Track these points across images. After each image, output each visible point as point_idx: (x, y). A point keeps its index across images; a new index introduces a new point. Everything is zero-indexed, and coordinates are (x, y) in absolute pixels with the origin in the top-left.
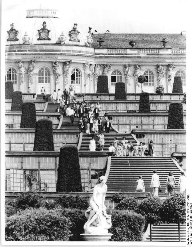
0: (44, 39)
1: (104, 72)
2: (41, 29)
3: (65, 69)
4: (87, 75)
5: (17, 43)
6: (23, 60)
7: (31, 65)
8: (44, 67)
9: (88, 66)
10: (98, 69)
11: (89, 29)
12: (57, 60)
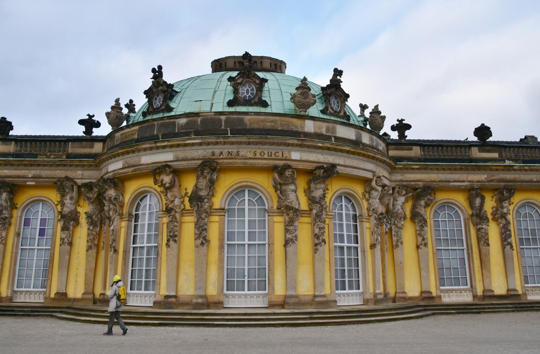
0: (247, 102)
1: (417, 210)
2: (238, 74)
3: (313, 194)
4: (377, 217)
7: (201, 180)
8: (247, 186)
11: (359, 109)
12: (289, 163)
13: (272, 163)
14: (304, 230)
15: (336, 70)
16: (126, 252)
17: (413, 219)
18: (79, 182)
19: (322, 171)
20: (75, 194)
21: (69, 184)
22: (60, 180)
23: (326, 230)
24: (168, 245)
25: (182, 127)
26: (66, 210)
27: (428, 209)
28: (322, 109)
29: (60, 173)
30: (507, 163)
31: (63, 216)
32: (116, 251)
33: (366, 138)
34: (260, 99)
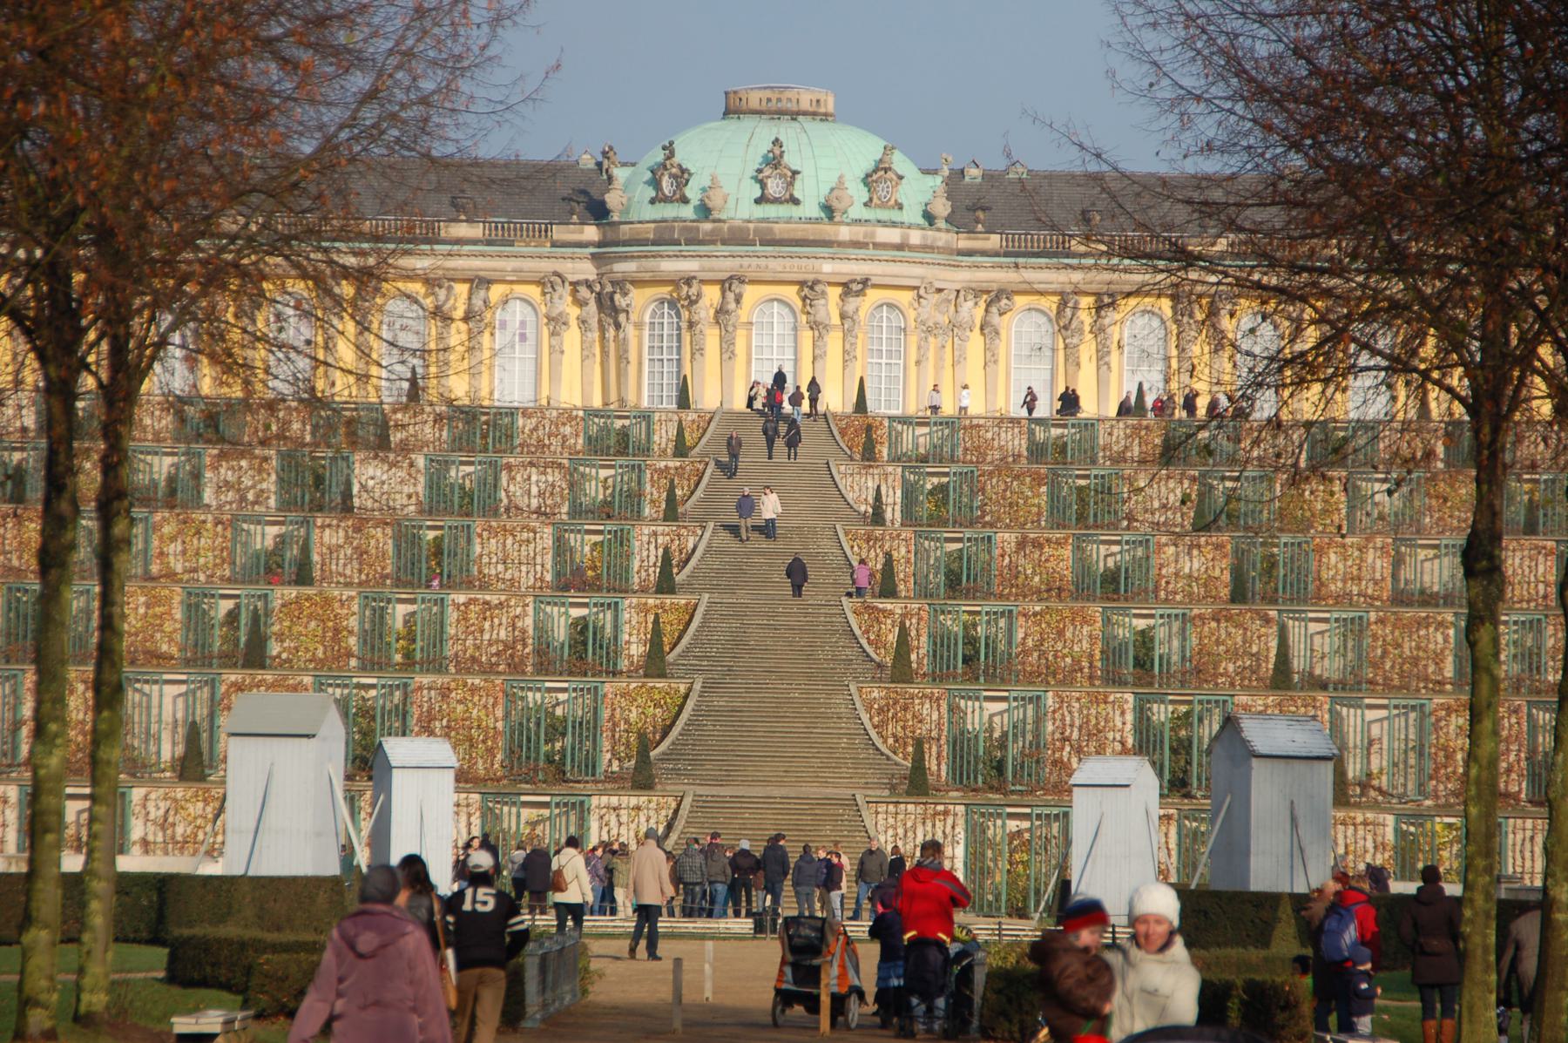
0: (776, 201)
6: (701, 276)
12: (820, 277)
13: (800, 277)
25: (706, 233)
28: (866, 199)
29: (547, 266)
31: (550, 319)
33: (915, 237)
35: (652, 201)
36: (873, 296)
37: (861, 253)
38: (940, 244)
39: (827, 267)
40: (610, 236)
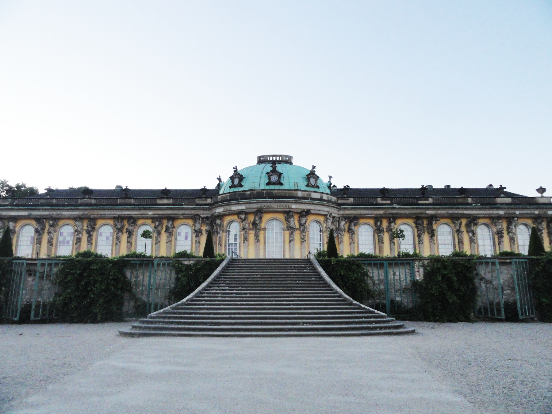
0: (274, 184)
5: (241, 189)
9: (331, 219)
10: (343, 223)
11: (328, 178)
14: (297, 235)
15: (313, 166)
16: (225, 246)
17: (348, 231)
18: (202, 216)
19: (304, 213)
20: (200, 222)
21: (198, 217)
22: (194, 215)
23: (306, 236)
24: (244, 242)
26: (197, 229)
27: (356, 227)
29: (194, 212)
30: (395, 206)
31: (196, 231)
32: (221, 245)
33: (325, 197)
34: (280, 182)
35: (230, 187)
36: (311, 218)
37: (307, 201)
38: (333, 200)
39: (294, 206)
40: (216, 200)
